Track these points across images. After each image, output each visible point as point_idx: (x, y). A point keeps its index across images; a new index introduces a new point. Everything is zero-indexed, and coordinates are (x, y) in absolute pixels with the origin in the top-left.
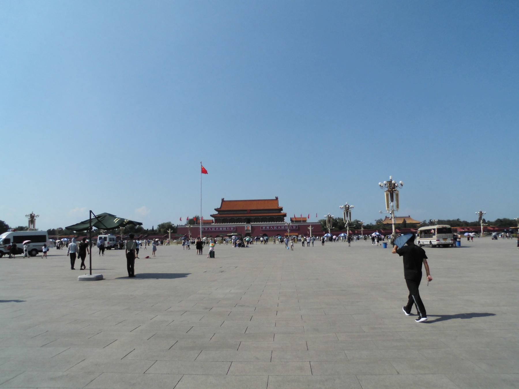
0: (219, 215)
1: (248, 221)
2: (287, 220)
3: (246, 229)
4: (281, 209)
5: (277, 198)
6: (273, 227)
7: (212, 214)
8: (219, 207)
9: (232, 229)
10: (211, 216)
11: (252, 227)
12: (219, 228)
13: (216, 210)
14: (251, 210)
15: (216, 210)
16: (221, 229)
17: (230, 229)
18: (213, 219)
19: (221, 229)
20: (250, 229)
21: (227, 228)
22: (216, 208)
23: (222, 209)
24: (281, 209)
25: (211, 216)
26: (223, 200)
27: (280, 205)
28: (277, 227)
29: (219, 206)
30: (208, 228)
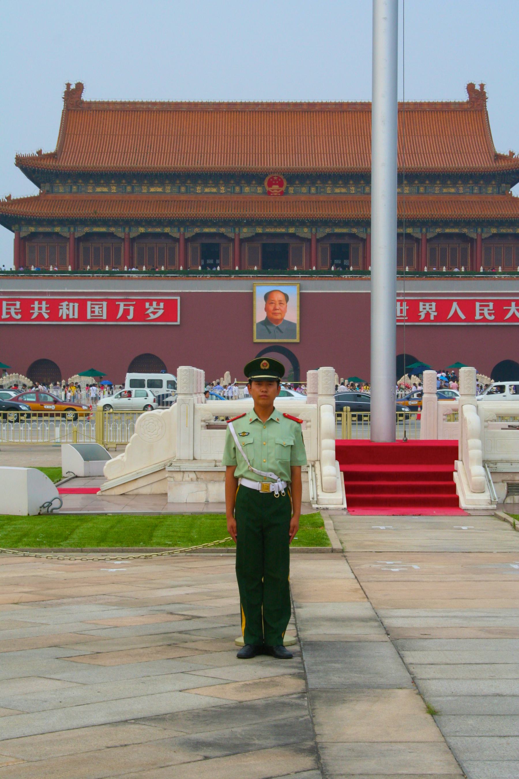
0: (44, 211)
1: (275, 260)
3: (260, 315)
5: (477, 96)
6: (468, 306)
8: (50, 146)
9: (155, 312)
11: (303, 297)
12: (54, 306)
13: (29, 167)
15: (29, 167)
16: (69, 311)
17: (141, 312)
19: (69, 311)
20: (292, 314)
22: (29, 150)
26: (73, 95)
28: (500, 307)
29: (45, 138)
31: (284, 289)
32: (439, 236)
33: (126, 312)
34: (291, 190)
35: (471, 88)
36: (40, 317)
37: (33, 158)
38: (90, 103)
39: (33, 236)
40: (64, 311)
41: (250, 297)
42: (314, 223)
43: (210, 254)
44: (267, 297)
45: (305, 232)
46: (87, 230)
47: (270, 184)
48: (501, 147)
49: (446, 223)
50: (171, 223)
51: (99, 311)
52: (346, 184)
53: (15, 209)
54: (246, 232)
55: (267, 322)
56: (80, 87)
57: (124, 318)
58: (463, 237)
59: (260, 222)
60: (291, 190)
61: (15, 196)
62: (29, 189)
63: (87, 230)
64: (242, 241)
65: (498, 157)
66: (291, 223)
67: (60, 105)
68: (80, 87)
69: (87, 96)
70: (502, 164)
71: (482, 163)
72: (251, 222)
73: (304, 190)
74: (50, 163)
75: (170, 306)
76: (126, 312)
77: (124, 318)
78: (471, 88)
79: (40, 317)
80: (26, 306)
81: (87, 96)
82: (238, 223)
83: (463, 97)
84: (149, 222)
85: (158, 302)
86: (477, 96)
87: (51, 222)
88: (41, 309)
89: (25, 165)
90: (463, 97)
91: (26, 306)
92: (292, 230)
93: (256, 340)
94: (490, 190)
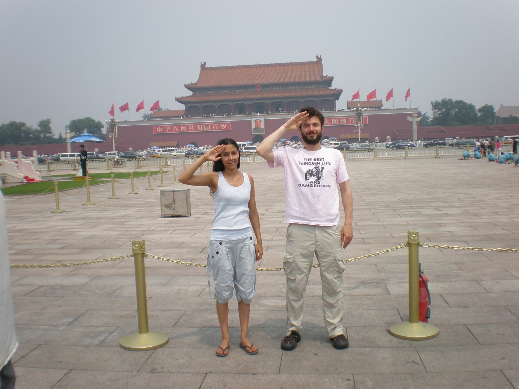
0: (193, 99)
2: (341, 104)
3: (253, 127)
4: (329, 81)
5: (319, 59)
7: (180, 96)
10: (179, 100)
11: (265, 121)
12: (195, 126)
13: (188, 87)
14: (264, 86)
18: (182, 107)
19: (199, 128)
20: (262, 126)
21: (212, 126)
22: (188, 82)
23: (199, 85)
24: (329, 81)
25: (179, 100)
26: (203, 66)
27: (327, 72)
30: (172, 127)
31: (260, 119)
32: (306, 101)
33: (215, 127)
34: (263, 90)
35: (317, 57)
36: (191, 130)
37: (189, 85)
38: (208, 68)
39: (191, 107)
40: (198, 128)
41: (250, 121)
42: (269, 99)
43: (241, 108)
44: (255, 121)
45: (267, 102)
46: (205, 104)
47: (257, 88)
48: (324, 75)
49: (308, 97)
50: (228, 101)
51: (208, 128)
52: (279, 87)
53: (184, 100)
54: (250, 102)
55: (255, 129)
56: (205, 63)
57: (215, 129)
58: (313, 100)
59: (254, 99)
60: (263, 90)
61: (185, 95)
62: (190, 93)
63: (205, 104)
64: (250, 105)
65: (323, 77)
66: (263, 99)
67: (200, 69)
68: (205, 63)
69: (207, 66)
70: (324, 79)
71: (318, 79)
72: (251, 100)
73: (267, 89)
74: (195, 86)
75: (228, 125)
76: (215, 127)
77: (215, 129)
78: (317, 57)
79: (191, 130)
80: (188, 127)
81: (207, 66)
82: (247, 100)
83: (315, 60)
84: (223, 101)
85: (224, 124)
86: (319, 60)
87: (195, 103)
88: (191, 128)
89: (188, 87)
90: (315, 60)
91: (188, 127)
92: (263, 101)
93: (253, 134)
94: (321, 86)
